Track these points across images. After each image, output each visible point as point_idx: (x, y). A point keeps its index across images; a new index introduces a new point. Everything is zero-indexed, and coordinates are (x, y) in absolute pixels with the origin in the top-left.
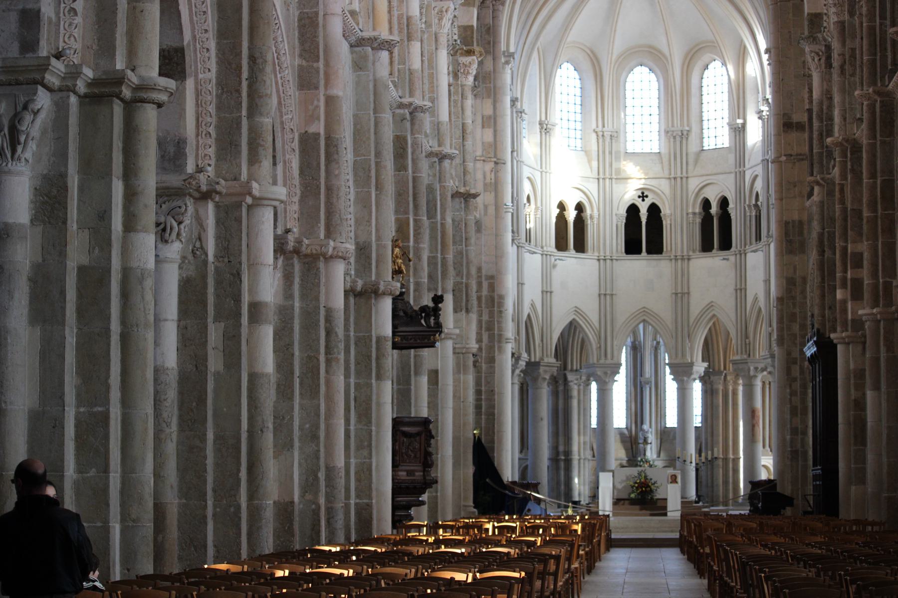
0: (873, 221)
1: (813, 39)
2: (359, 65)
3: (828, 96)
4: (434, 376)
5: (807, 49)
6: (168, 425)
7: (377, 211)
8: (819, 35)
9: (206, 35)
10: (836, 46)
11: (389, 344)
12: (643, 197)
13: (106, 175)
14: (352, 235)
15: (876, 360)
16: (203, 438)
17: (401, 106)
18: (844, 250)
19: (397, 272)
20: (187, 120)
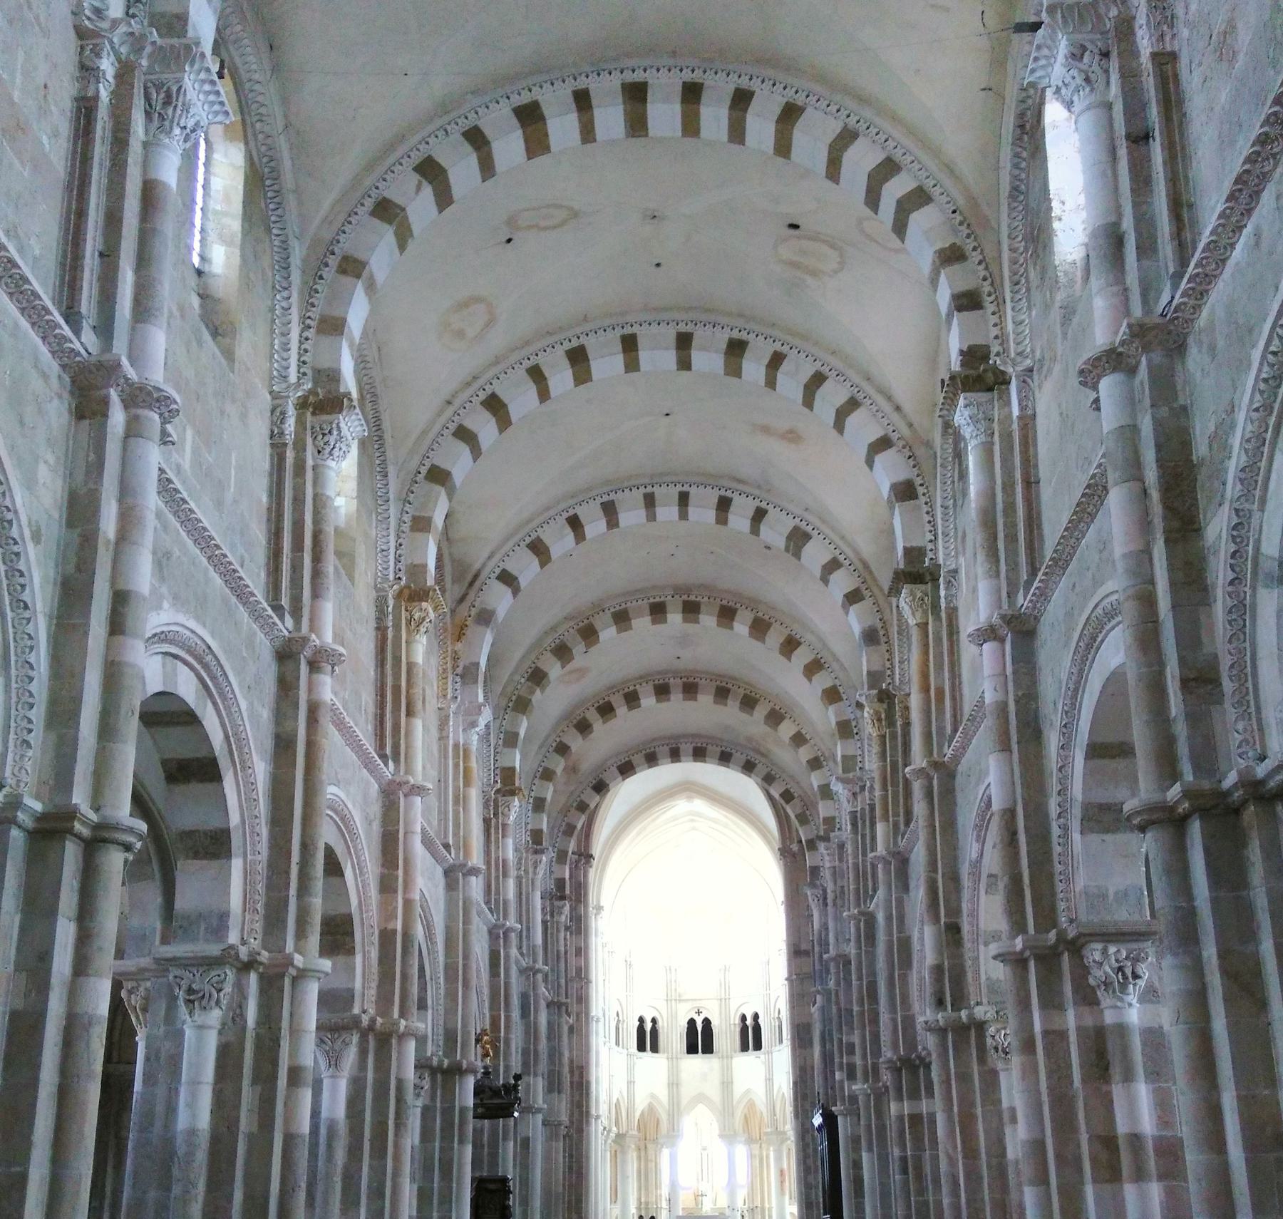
0: (862, 1013)
1: (813, 885)
2: (451, 885)
3: (825, 927)
4: (526, 1144)
5: (809, 893)
6: (194, 1186)
7: (463, 1003)
8: (818, 882)
9: (257, 821)
10: (830, 887)
11: (471, 1114)
12: (699, 1013)
13: (51, 913)
14: (441, 1022)
15: (869, 1127)
16: (230, 1199)
17: (495, 926)
18: (841, 1040)
19: (486, 1055)
20: (232, 896)
